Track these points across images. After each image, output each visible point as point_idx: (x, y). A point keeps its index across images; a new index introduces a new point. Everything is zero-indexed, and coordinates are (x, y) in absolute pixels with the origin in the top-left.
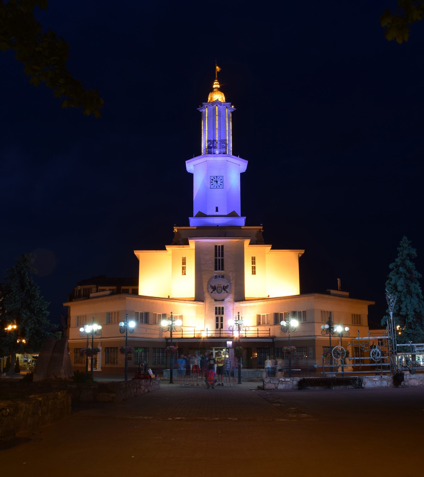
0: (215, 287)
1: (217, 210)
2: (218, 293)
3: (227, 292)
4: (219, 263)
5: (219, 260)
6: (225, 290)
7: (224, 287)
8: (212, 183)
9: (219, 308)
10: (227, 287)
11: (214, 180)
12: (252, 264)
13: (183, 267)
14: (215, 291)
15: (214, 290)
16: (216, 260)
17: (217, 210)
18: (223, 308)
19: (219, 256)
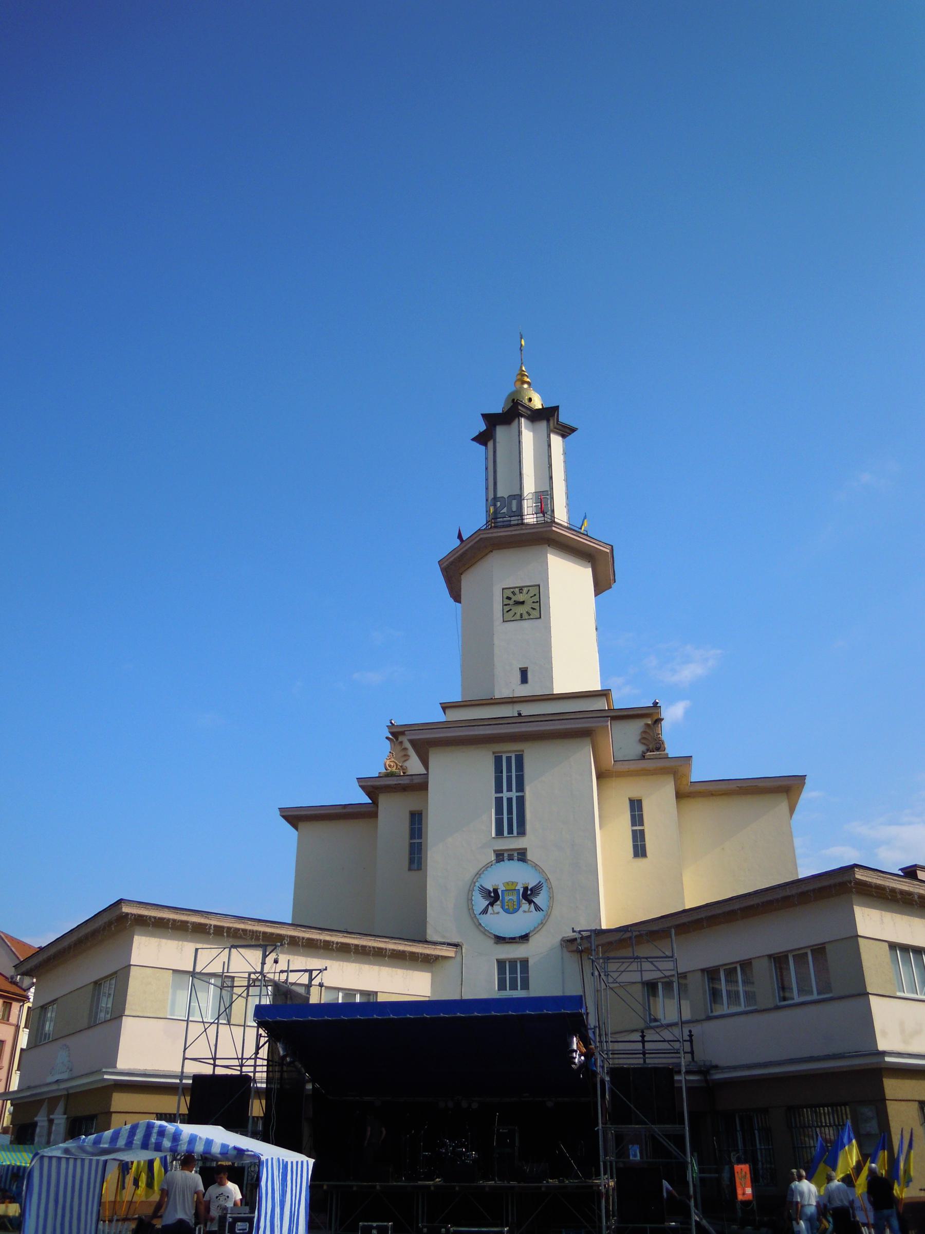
0: (495, 891)
1: (524, 679)
2: (507, 911)
3: (537, 908)
4: (510, 812)
5: (510, 800)
6: (530, 902)
7: (526, 889)
8: (507, 608)
9: (513, 962)
10: (536, 890)
11: (514, 598)
12: (633, 824)
13: (412, 846)
14: (497, 907)
15: (492, 904)
16: (499, 801)
17: (524, 679)
18: (525, 962)
19: (509, 789)
